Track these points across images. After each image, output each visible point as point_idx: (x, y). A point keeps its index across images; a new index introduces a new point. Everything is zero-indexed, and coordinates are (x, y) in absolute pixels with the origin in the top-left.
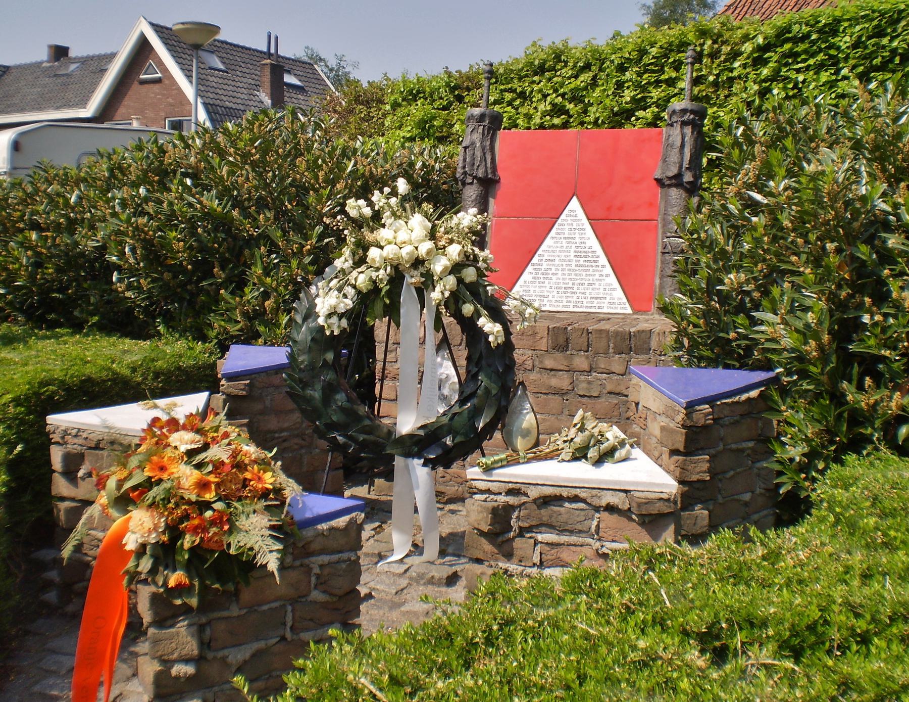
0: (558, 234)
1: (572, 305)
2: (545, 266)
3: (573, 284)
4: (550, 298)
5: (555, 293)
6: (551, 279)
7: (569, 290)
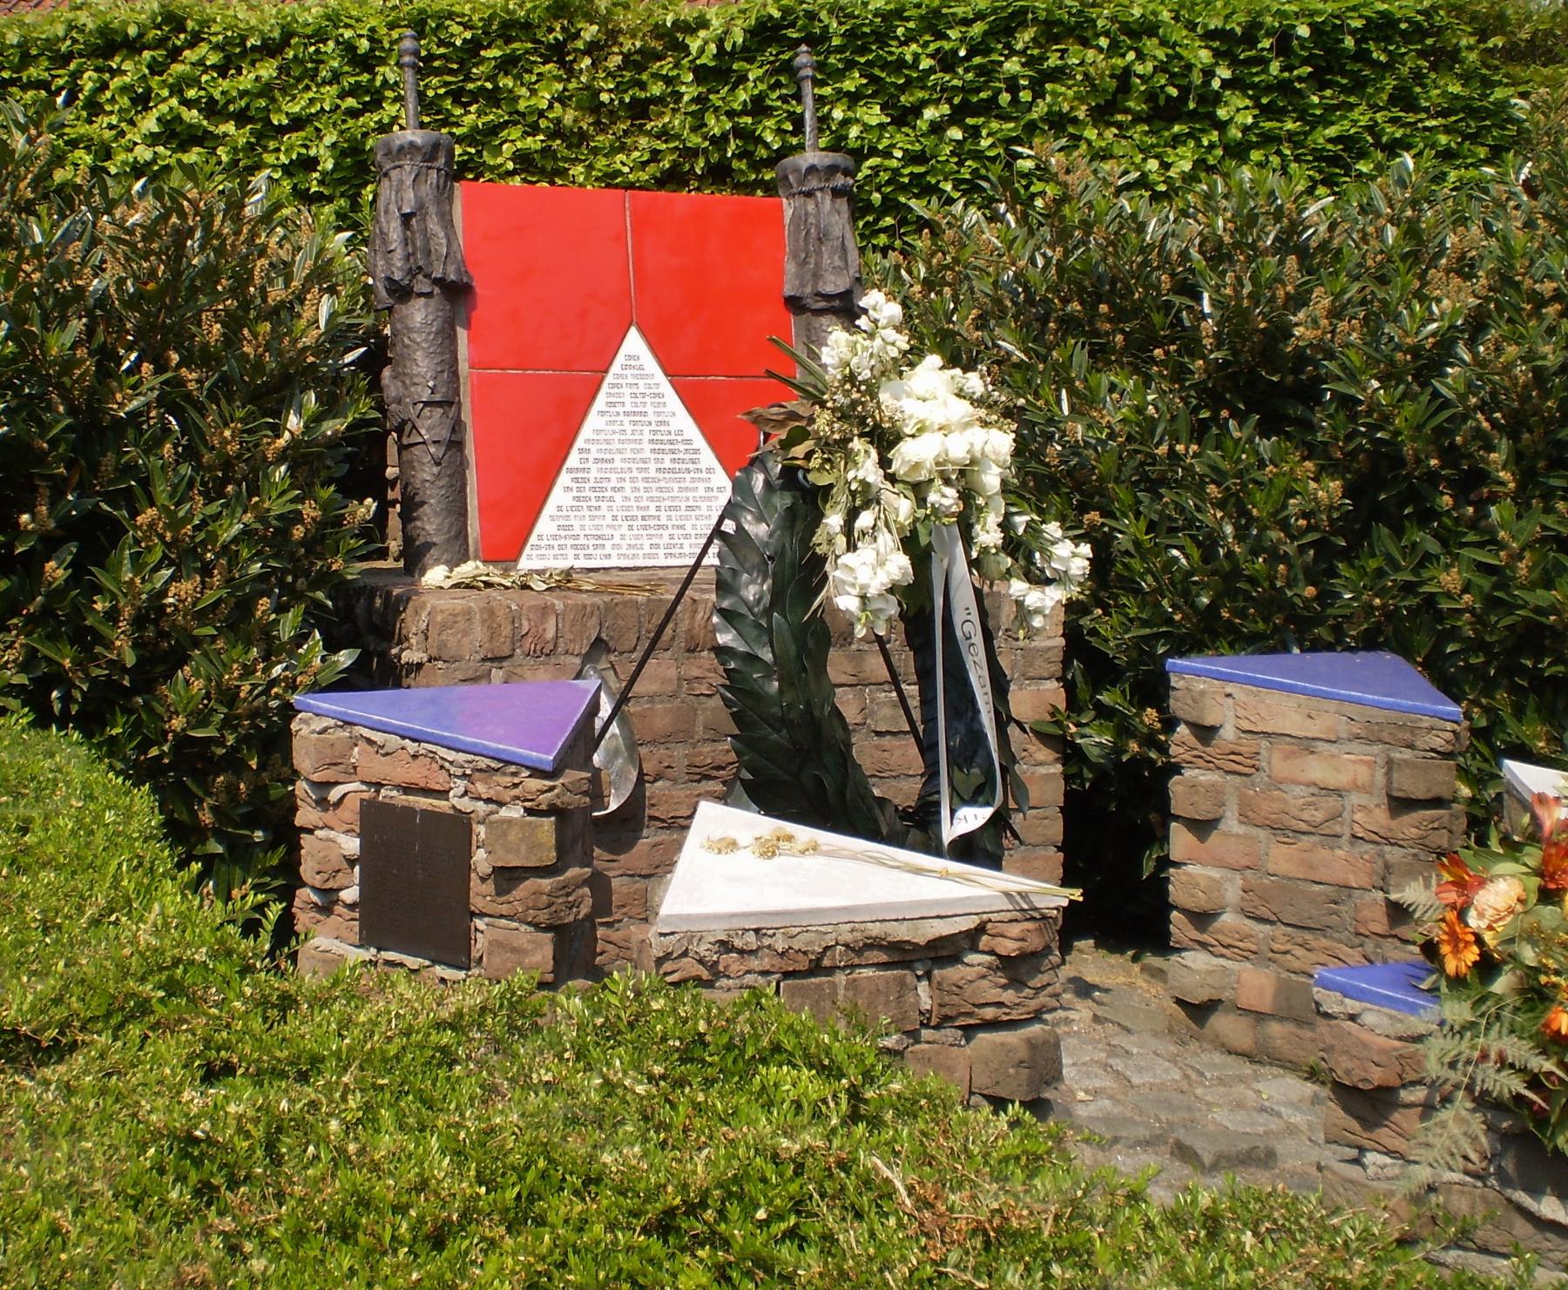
0: (610, 404)
1: (661, 552)
2: (593, 474)
3: (658, 508)
4: (617, 540)
5: (624, 530)
6: (611, 499)
7: (652, 523)
